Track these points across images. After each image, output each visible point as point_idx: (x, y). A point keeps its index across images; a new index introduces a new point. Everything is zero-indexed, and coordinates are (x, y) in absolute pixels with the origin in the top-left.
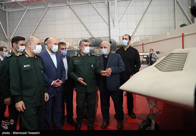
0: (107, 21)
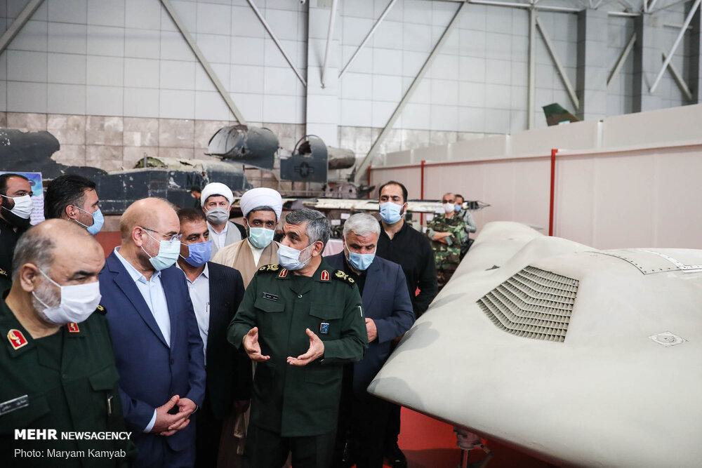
0: (298, 64)
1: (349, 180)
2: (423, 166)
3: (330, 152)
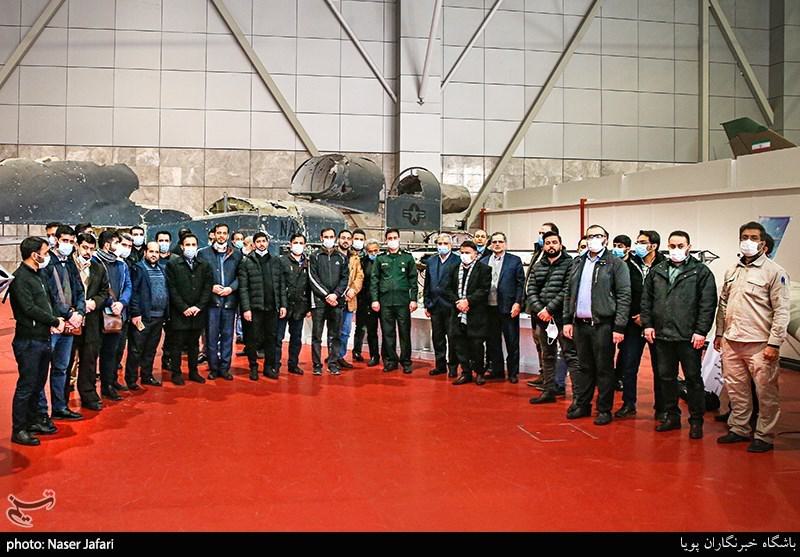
0: (385, 73)
1: (459, 228)
2: (582, 206)
3: (444, 191)
